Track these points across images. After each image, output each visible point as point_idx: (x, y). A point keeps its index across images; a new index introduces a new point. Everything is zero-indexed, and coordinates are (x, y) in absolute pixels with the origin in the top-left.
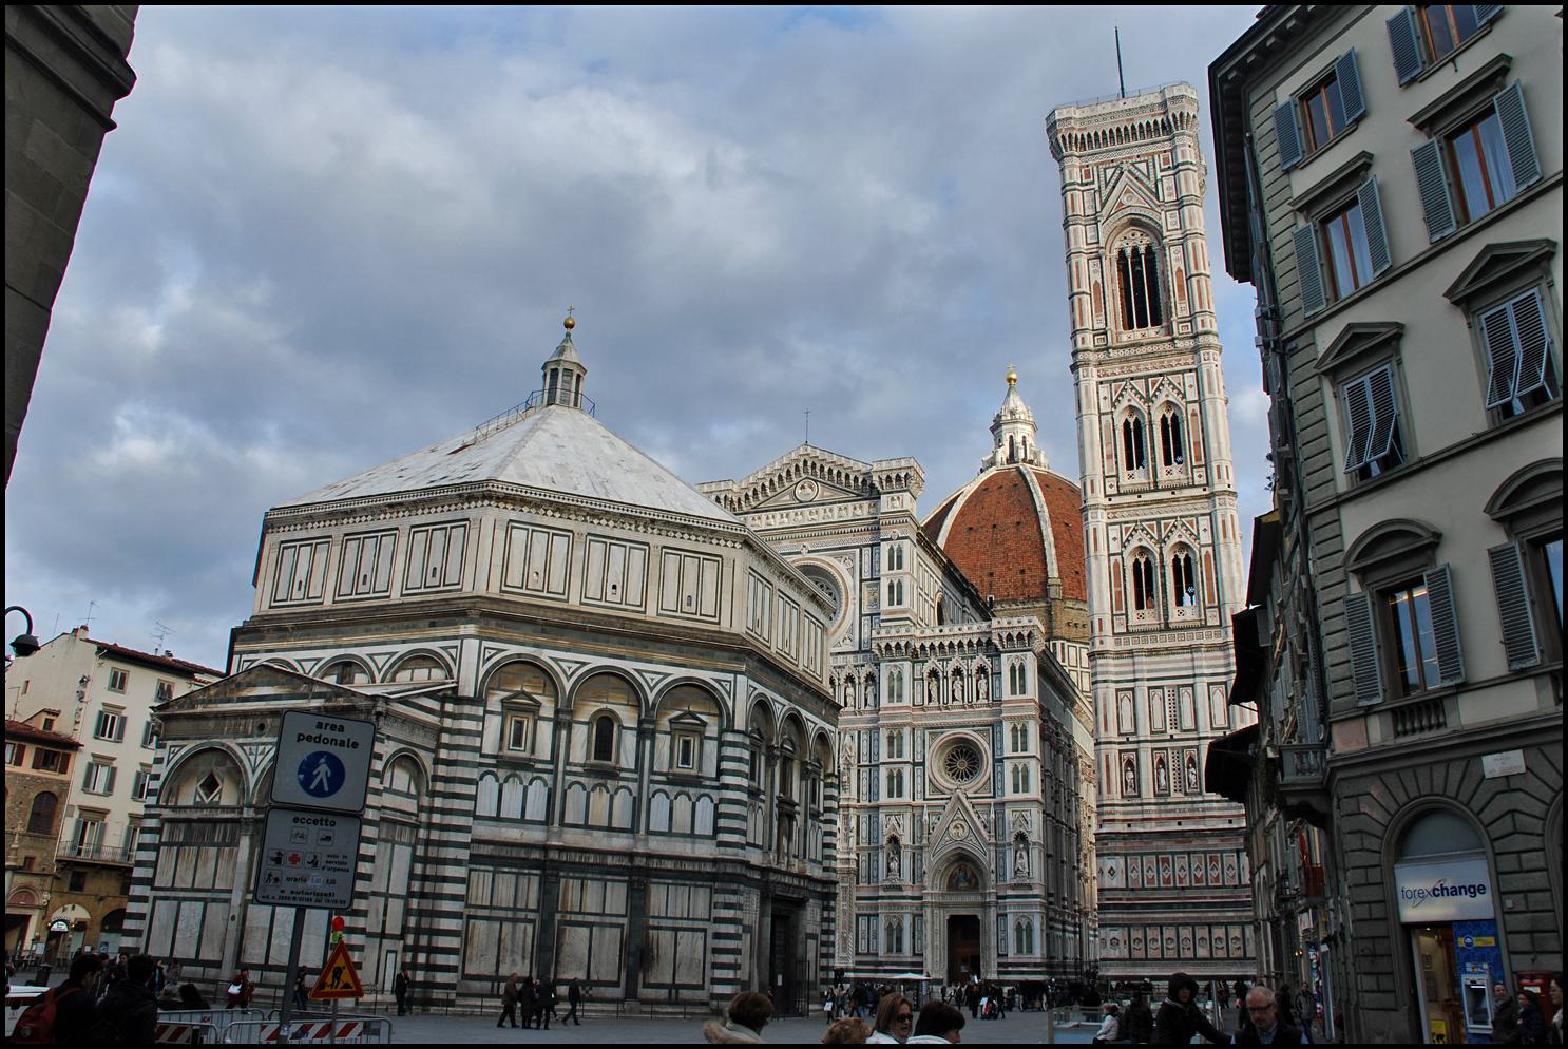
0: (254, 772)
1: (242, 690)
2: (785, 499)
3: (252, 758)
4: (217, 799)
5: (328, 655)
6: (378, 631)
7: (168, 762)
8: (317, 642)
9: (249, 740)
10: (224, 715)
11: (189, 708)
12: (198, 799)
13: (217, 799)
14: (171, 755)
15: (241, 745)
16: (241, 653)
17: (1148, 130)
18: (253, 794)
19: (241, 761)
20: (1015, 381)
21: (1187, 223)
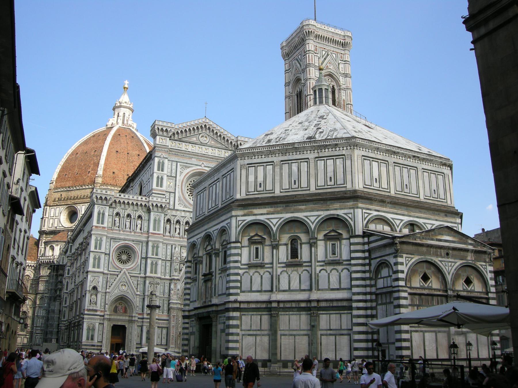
0: (449, 274)
1: (437, 236)
2: (193, 139)
3: (447, 268)
4: (430, 285)
5: (406, 219)
6: (424, 213)
7: (406, 265)
8: (399, 212)
9: (443, 259)
10: (431, 246)
11: (413, 239)
12: (421, 284)
13: (430, 285)
14: (407, 262)
15: (441, 261)
16: (362, 208)
17: (336, 42)
18: (451, 284)
19: (442, 269)
20: (127, 88)
21: (348, 84)
